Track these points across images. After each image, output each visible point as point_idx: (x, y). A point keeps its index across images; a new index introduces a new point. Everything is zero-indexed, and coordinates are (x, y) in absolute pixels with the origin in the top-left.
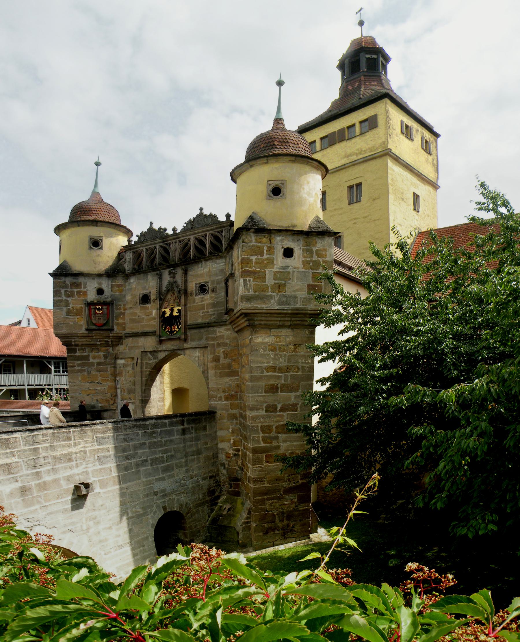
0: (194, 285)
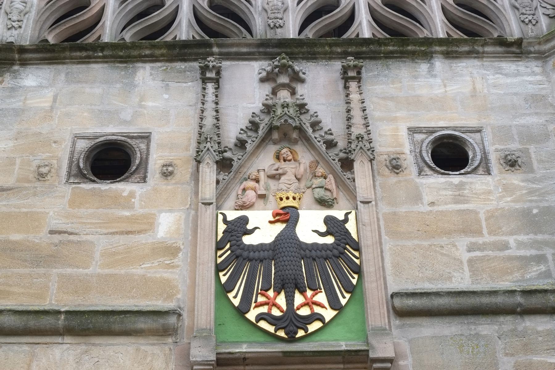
0: (403, 133)
